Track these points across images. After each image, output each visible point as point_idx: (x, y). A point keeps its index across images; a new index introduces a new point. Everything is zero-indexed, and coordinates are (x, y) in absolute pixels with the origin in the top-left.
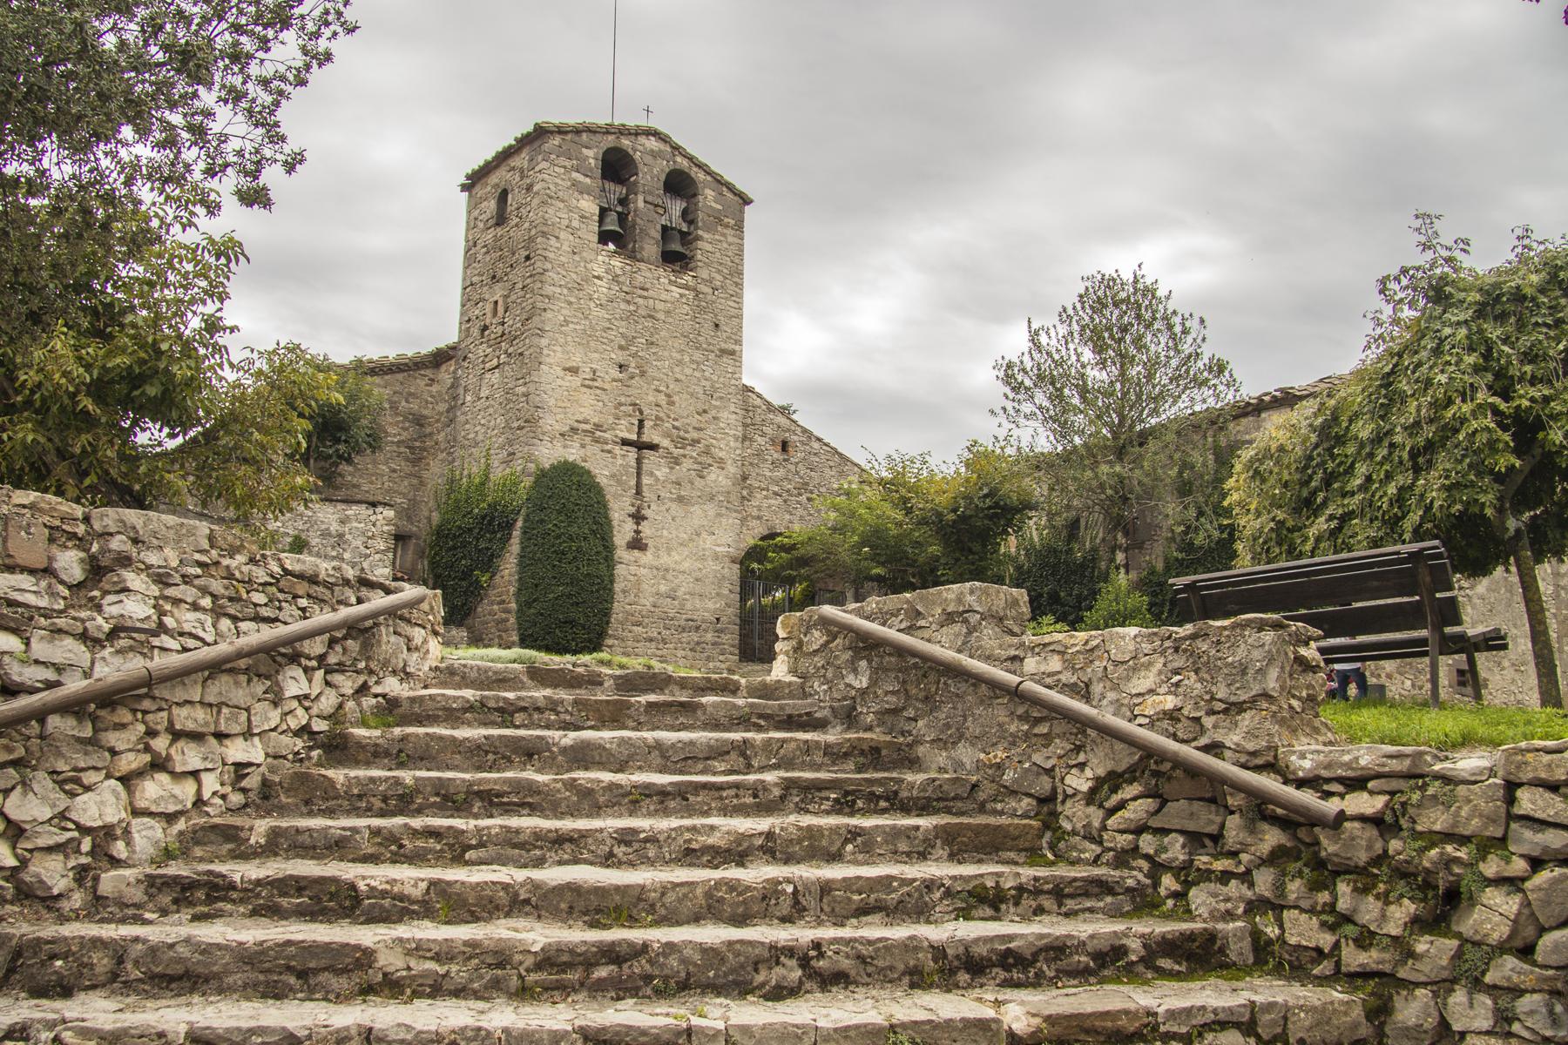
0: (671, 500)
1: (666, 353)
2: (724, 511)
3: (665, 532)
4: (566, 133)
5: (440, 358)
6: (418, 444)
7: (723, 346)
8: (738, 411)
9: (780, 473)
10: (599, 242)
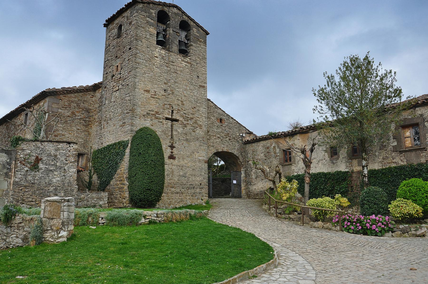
1: (181, 86)
2: (202, 144)
5: (96, 87)
6: (87, 119)
7: (200, 84)
8: (206, 108)
9: (220, 130)
10: (157, 44)
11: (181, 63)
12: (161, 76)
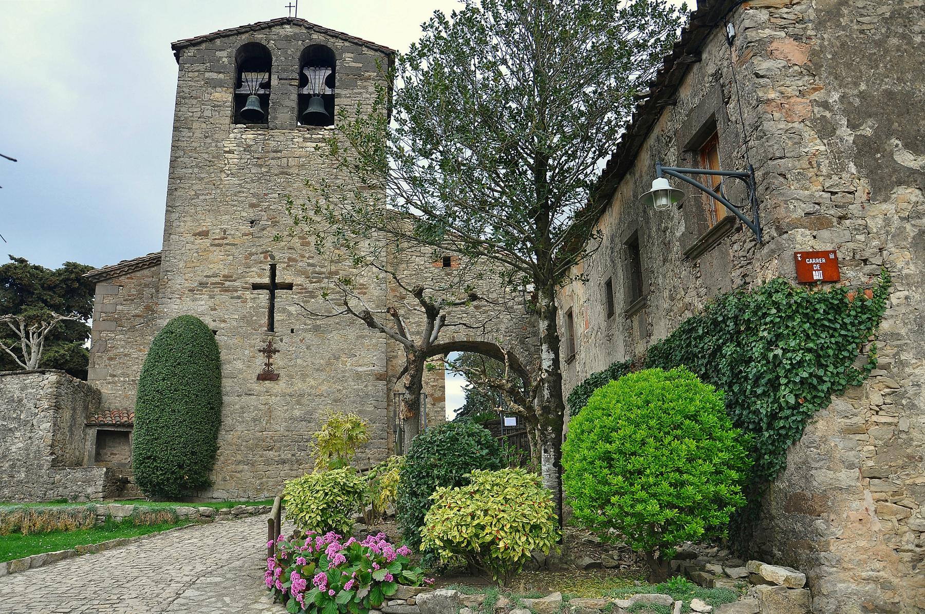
0: (305, 330)
3: (299, 361)
4: (199, 43)
11: (302, 148)
12: (240, 192)
